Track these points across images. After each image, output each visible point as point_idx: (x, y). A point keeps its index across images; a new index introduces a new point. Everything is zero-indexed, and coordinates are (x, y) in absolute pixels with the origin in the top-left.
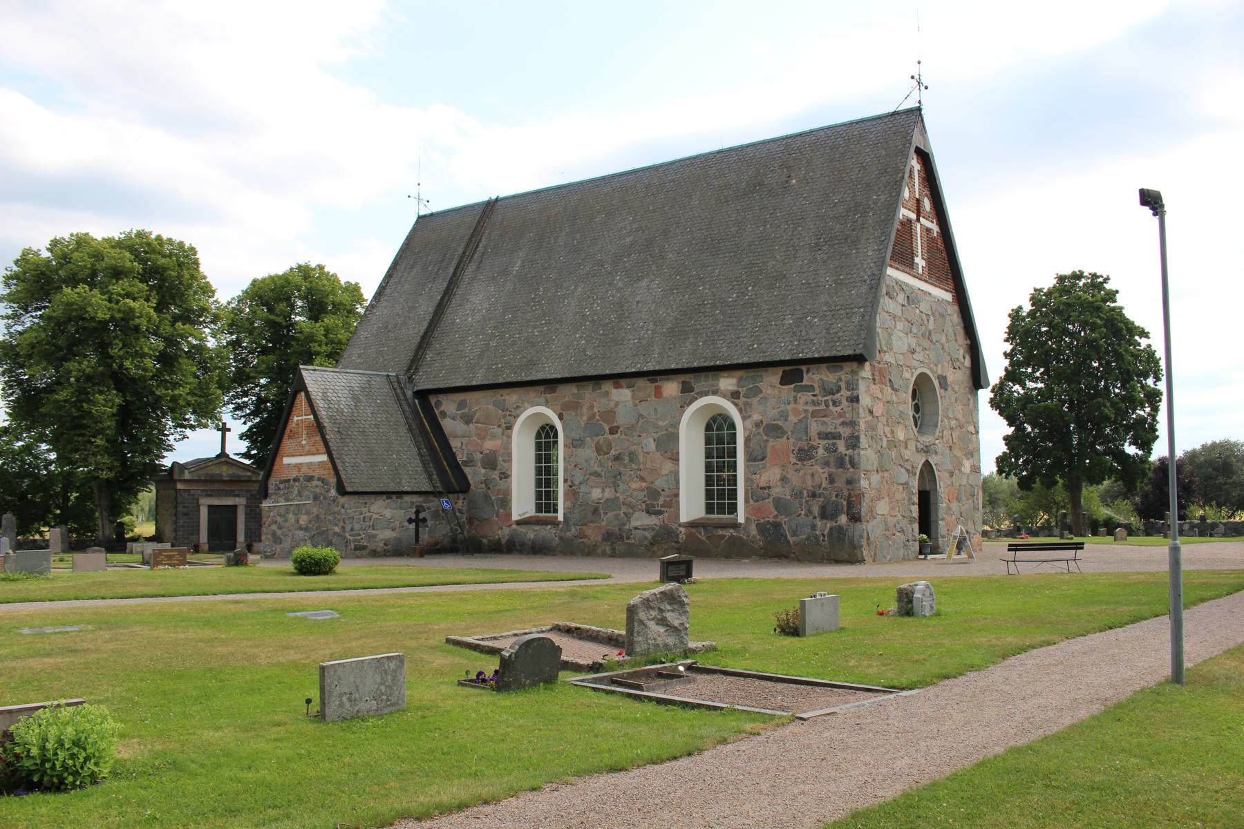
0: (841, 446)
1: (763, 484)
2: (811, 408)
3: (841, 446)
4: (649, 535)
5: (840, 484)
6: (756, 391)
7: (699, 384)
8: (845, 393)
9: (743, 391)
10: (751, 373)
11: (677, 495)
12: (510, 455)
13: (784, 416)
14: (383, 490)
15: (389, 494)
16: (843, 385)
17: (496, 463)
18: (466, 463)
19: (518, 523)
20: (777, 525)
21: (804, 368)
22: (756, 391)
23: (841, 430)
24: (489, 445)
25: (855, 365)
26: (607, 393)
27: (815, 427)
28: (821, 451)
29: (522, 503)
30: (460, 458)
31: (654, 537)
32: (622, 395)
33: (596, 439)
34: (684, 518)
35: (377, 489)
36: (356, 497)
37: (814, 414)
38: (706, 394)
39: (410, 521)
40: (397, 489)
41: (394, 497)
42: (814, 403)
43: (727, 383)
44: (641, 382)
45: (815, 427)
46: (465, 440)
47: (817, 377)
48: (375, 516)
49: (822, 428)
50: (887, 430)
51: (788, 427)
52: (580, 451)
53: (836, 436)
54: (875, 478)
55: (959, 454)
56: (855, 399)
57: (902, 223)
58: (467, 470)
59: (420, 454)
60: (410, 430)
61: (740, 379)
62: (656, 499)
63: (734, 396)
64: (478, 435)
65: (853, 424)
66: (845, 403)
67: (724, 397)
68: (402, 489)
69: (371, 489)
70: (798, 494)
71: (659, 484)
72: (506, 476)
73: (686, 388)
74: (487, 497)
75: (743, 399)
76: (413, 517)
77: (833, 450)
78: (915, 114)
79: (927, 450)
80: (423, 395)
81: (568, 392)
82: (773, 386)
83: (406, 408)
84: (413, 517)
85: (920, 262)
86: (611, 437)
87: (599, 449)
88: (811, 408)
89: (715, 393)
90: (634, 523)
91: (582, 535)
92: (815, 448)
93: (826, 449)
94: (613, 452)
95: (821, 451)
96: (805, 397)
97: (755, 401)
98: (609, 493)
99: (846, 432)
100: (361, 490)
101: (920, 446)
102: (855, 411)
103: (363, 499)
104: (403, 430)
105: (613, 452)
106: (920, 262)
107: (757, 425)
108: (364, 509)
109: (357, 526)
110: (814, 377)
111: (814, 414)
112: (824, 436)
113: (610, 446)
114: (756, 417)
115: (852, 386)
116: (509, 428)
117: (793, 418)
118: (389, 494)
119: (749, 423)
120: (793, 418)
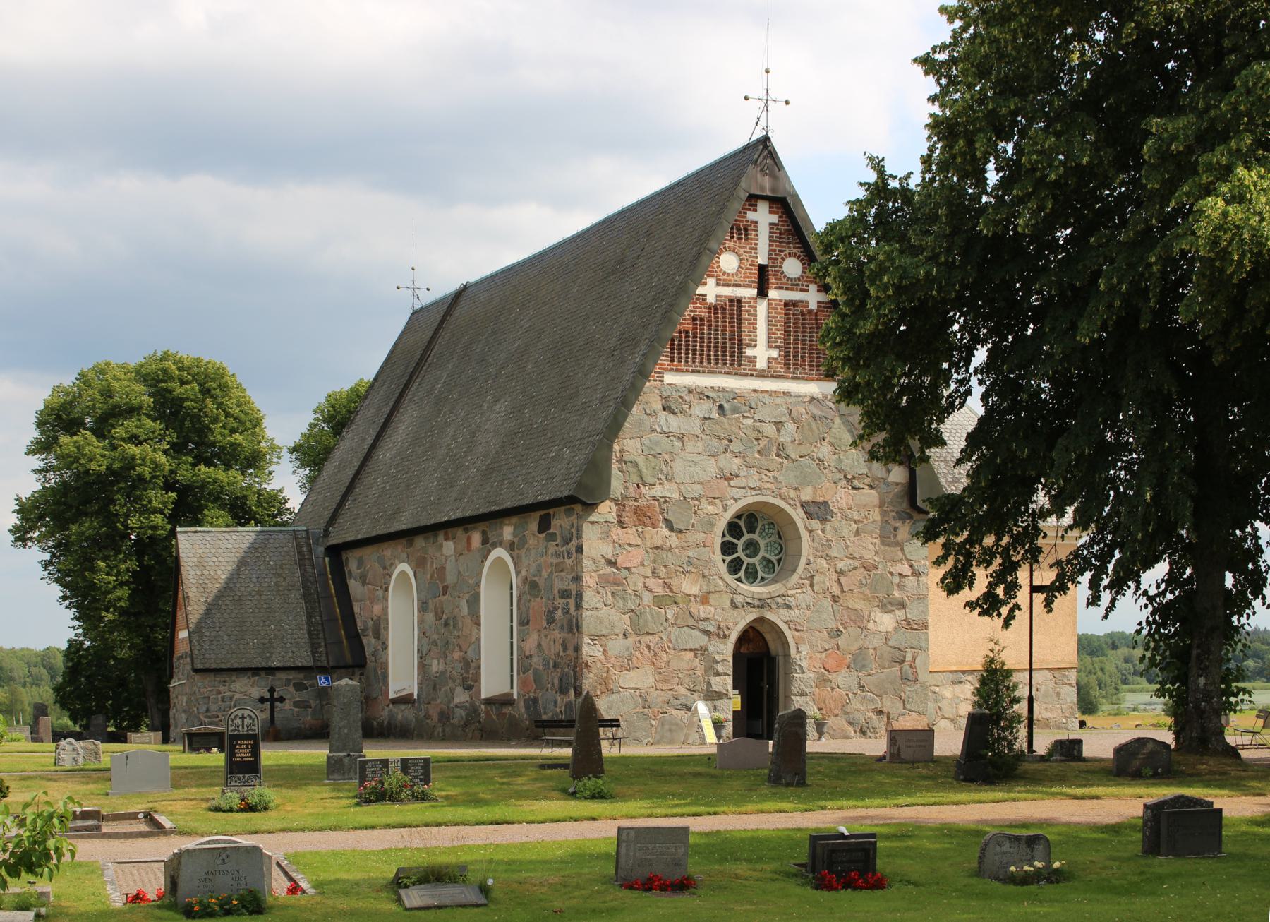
1: (528, 653)
2: (555, 561)
3: (572, 602)
4: (463, 713)
5: (570, 652)
6: (523, 541)
8: (575, 542)
9: (516, 540)
11: (479, 667)
12: (387, 620)
14: (245, 665)
15: (256, 671)
16: (574, 530)
17: (379, 628)
19: (395, 701)
20: (535, 700)
21: (551, 511)
24: (377, 609)
25: (578, 507)
26: (441, 546)
29: (402, 676)
30: (360, 626)
31: (467, 715)
32: (449, 547)
34: (483, 696)
35: (236, 666)
36: (212, 675)
39: (262, 700)
40: (264, 665)
41: (263, 674)
42: (557, 555)
43: (508, 532)
44: (460, 532)
45: (558, 585)
48: (237, 696)
50: (651, 583)
51: (542, 584)
54: (617, 645)
55: (858, 604)
56: (580, 550)
57: (714, 308)
58: (365, 640)
59: (309, 623)
60: (306, 595)
62: (468, 672)
63: (511, 547)
65: (577, 579)
68: (270, 664)
69: (228, 666)
70: (546, 665)
71: (471, 654)
72: (385, 647)
74: (375, 670)
76: (267, 695)
77: (566, 611)
78: (761, 152)
79: (763, 603)
80: (336, 552)
81: (420, 542)
83: (309, 569)
84: (267, 695)
85: (761, 353)
88: (555, 561)
90: (457, 700)
91: (427, 716)
92: (556, 609)
95: (559, 612)
96: (552, 548)
97: (523, 552)
98: (441, 667)
99: (573, 587)
100: (214, 666)
101: (739, 600)
103: (224, 676)
104: (296, 596)
106: (761, 353)
108: (222, 688)
109: (214, 707)
110: (560, 522)
114: (524, 573)
116: (387, 589)
117: (545, 574)
118: (256, 671)
120: (545, 574)
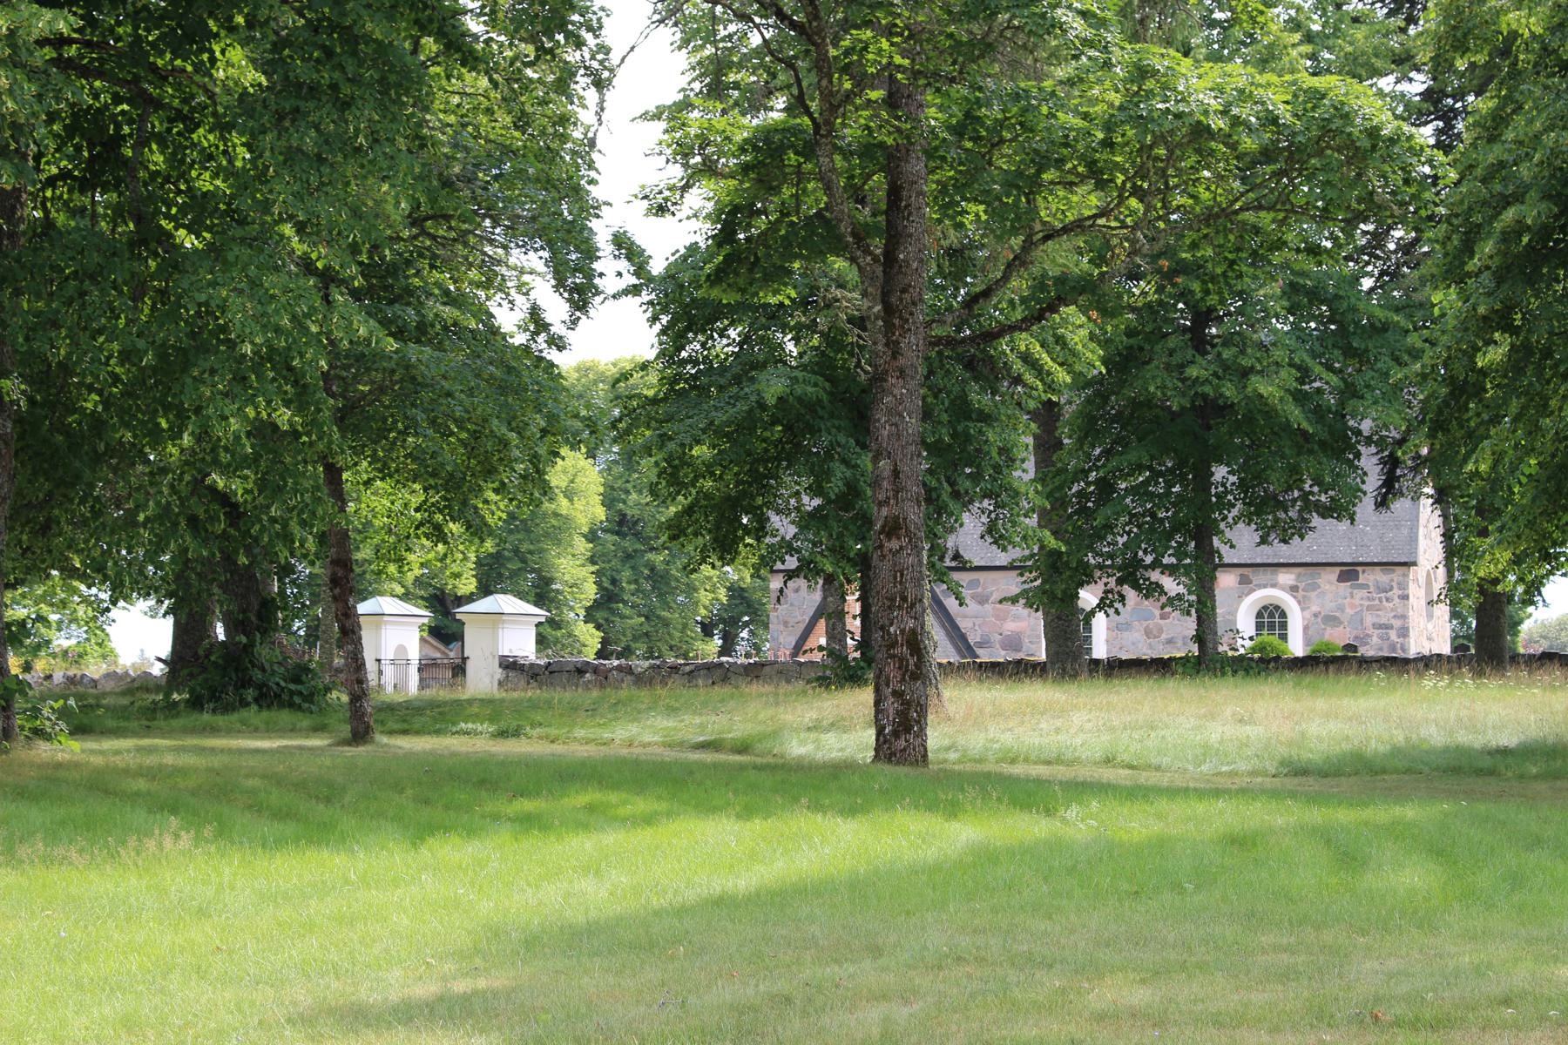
0: (1393, 635)
2: (1366, 603)
3: (1393, 635)
7: (1258, 577)
8: (1396, 592)
9: (1301, 586)
10: (1310, 570)
13: (1341, 609)
18: (981, 645)
22: (1315, 587)
23: (1393, 622)
27: (1369, 619)
28: (1375, 639)
33: (1145, 624)
37: (1369, 608)
38: (1265, 586)
43: (1286, 578)
45: (1369, 619)
46: (978, 621)
47: (1372, 577)
49: (1376, 620)
51: (1344, 618)
52: (1126, 634)
53: (1388, 627)
56: (1405, 597)
61: (1299, 575)
63: (1293, 589)
64: (997, 617)
65: (1404, 617)
66: (1396, 600)
67: (1283, 589)
73: (1244, 581)
75: (1301, 593)
82: (1331, 583)
86: (1162, 622)
87: (1148, 633)
88: (1366, 603)
89: (1274, 586)
93: (1381, 638)
94: (1164, 636)
95: (1375, 639)
97: (1313, 595)
102: (1406, 606)
105: (1164, 636)
107: (1316, 615)
110: (1368, 577)
111: (1369, 608)
112: (1381, 626)
113: (1161, 630)
114: (1315, 609)
115: (1403, 586)
117: (1349, 611)
119: (1307, 614)
120: (1349, 611)
